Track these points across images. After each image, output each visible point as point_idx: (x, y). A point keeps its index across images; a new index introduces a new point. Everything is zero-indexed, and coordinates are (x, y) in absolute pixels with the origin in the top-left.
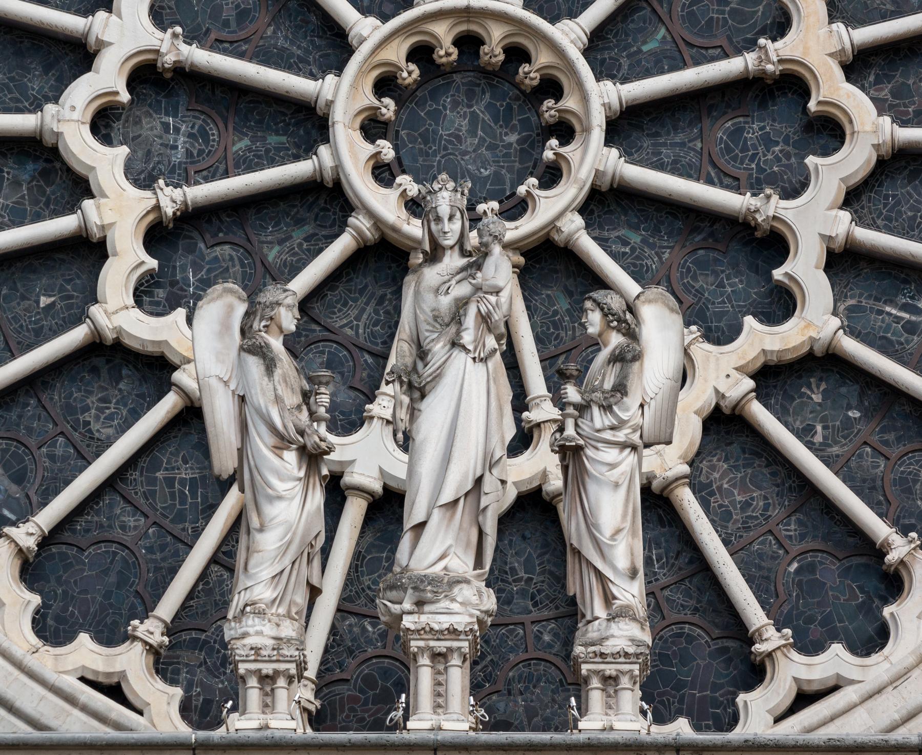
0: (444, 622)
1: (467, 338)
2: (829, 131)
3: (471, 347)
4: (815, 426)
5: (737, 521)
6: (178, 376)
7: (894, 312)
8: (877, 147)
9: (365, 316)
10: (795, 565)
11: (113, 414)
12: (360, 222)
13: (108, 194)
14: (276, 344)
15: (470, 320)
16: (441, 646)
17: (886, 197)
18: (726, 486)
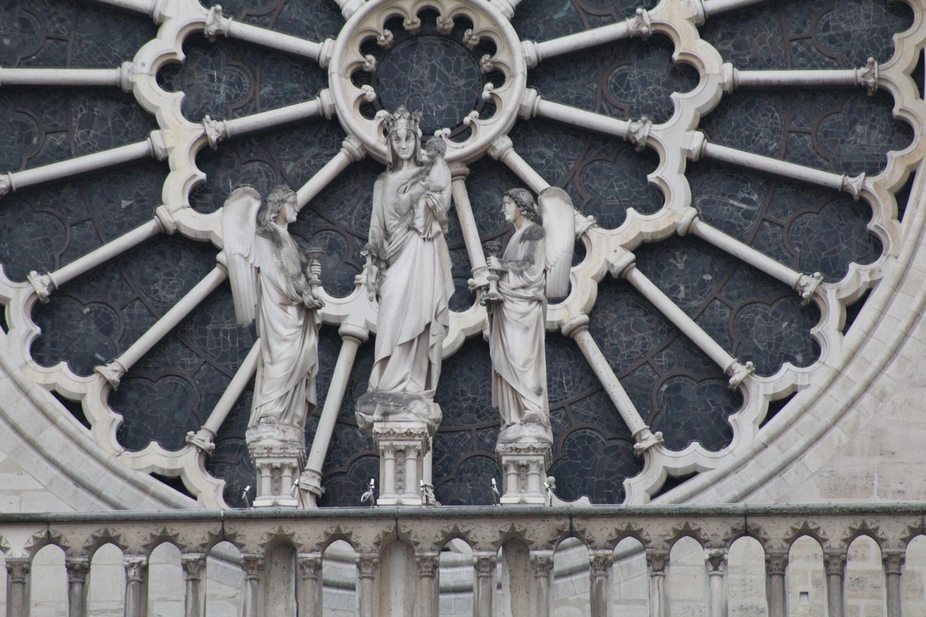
0: (404, 427)
9: (356, 212)
12: (350, 144)
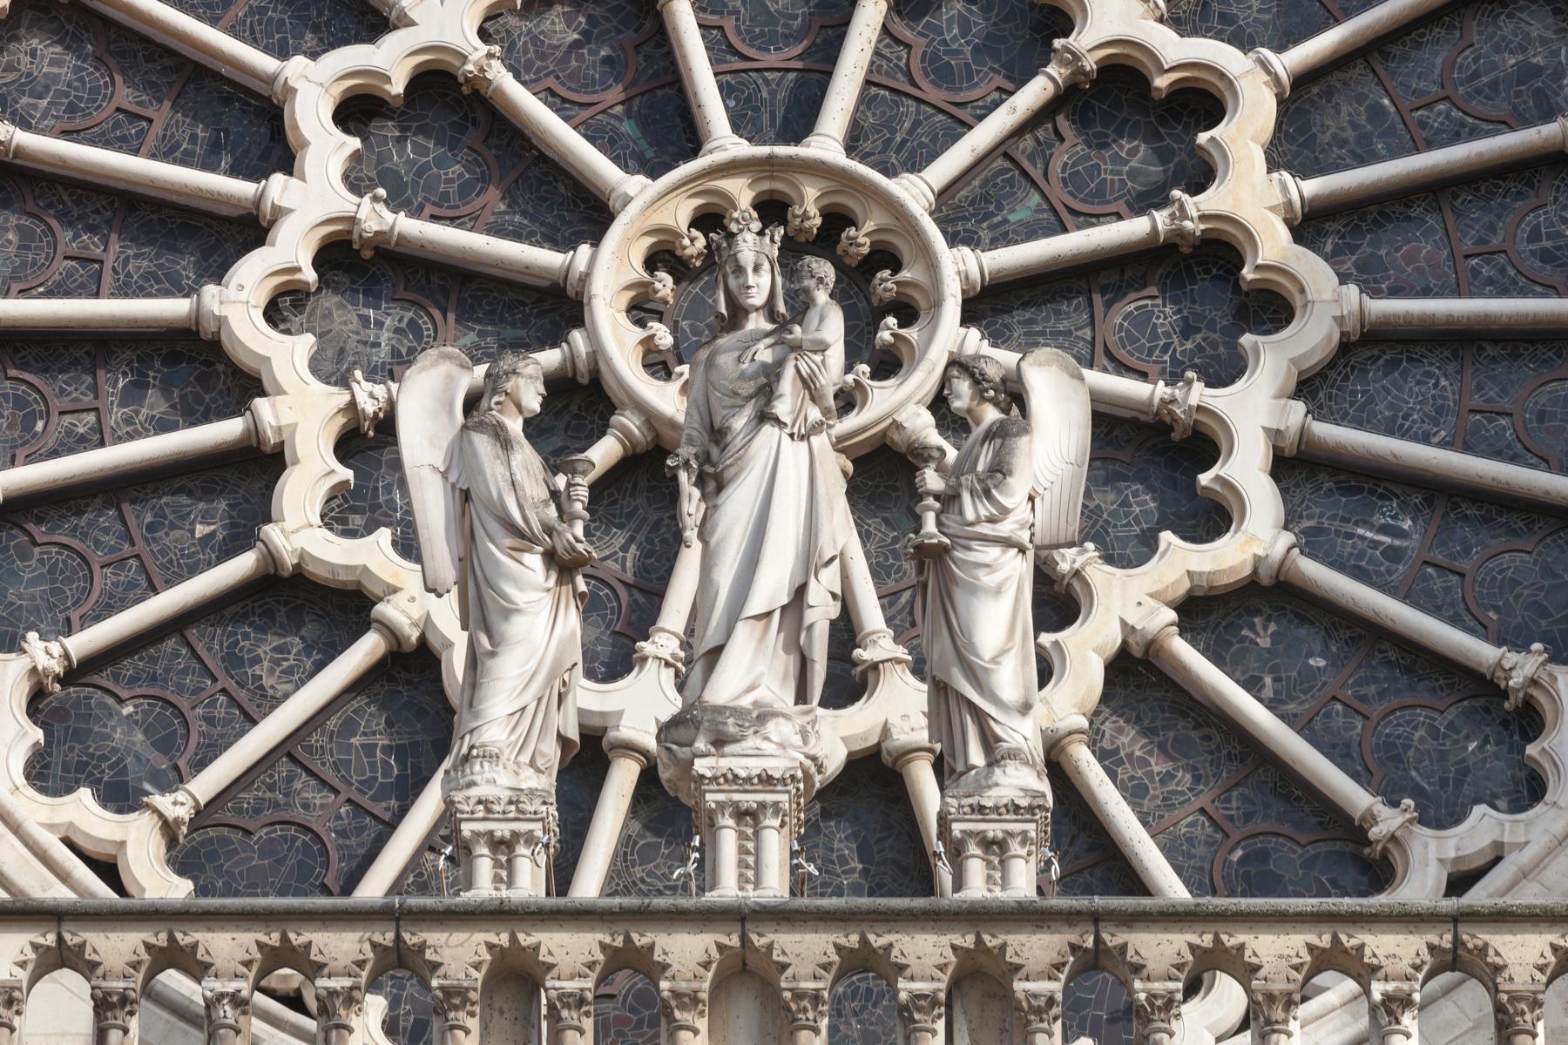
0: (755, 766)
1: (782, 408)
2: (1272, 307)
3: (787, 419)
5: (1154, 797)
6: (384, 610)
7: (1369, 534)
8: (1340, 320)
10: (1239, 853)
11: (292, 667)
13: (285, 387)
14: (515, 425)
15: (787, 384)
16: (749, 799)
17: (1354, 393)
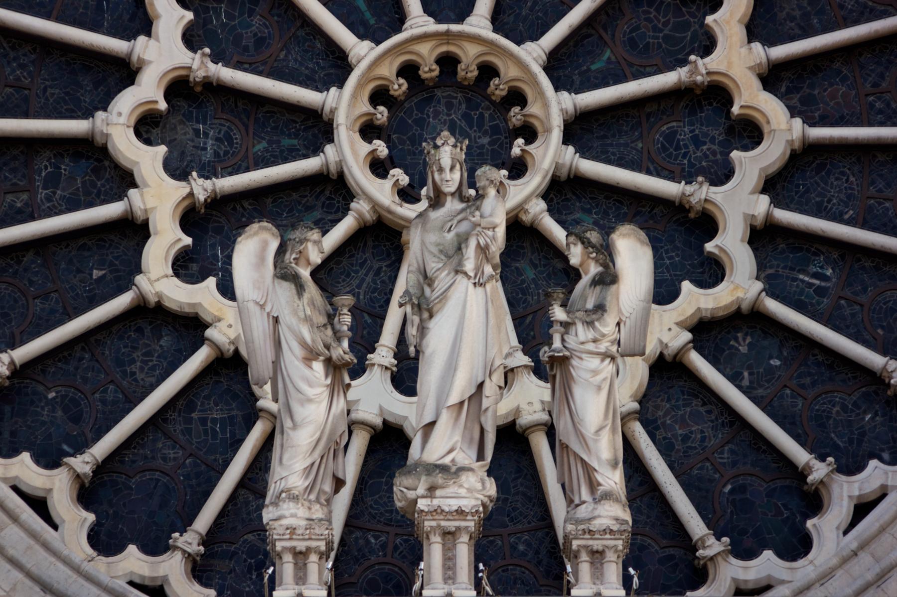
4: (742, 373)
9: (365, 285)
18: (668, 422)
